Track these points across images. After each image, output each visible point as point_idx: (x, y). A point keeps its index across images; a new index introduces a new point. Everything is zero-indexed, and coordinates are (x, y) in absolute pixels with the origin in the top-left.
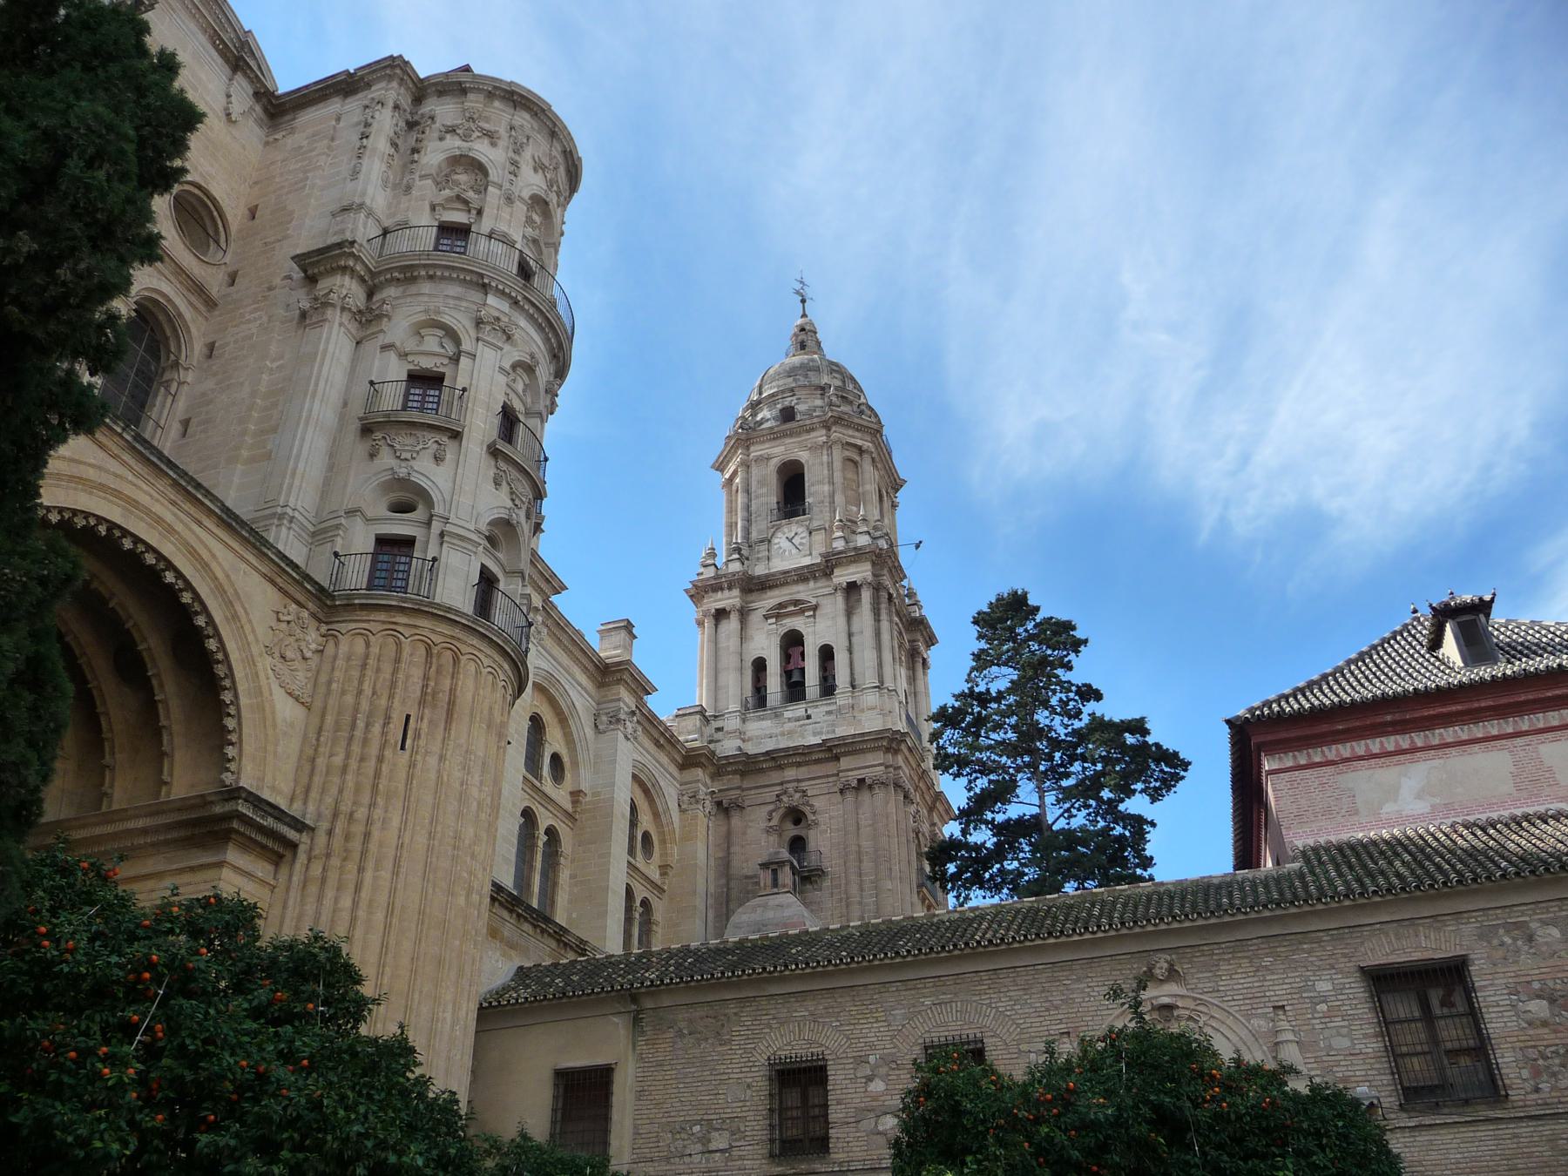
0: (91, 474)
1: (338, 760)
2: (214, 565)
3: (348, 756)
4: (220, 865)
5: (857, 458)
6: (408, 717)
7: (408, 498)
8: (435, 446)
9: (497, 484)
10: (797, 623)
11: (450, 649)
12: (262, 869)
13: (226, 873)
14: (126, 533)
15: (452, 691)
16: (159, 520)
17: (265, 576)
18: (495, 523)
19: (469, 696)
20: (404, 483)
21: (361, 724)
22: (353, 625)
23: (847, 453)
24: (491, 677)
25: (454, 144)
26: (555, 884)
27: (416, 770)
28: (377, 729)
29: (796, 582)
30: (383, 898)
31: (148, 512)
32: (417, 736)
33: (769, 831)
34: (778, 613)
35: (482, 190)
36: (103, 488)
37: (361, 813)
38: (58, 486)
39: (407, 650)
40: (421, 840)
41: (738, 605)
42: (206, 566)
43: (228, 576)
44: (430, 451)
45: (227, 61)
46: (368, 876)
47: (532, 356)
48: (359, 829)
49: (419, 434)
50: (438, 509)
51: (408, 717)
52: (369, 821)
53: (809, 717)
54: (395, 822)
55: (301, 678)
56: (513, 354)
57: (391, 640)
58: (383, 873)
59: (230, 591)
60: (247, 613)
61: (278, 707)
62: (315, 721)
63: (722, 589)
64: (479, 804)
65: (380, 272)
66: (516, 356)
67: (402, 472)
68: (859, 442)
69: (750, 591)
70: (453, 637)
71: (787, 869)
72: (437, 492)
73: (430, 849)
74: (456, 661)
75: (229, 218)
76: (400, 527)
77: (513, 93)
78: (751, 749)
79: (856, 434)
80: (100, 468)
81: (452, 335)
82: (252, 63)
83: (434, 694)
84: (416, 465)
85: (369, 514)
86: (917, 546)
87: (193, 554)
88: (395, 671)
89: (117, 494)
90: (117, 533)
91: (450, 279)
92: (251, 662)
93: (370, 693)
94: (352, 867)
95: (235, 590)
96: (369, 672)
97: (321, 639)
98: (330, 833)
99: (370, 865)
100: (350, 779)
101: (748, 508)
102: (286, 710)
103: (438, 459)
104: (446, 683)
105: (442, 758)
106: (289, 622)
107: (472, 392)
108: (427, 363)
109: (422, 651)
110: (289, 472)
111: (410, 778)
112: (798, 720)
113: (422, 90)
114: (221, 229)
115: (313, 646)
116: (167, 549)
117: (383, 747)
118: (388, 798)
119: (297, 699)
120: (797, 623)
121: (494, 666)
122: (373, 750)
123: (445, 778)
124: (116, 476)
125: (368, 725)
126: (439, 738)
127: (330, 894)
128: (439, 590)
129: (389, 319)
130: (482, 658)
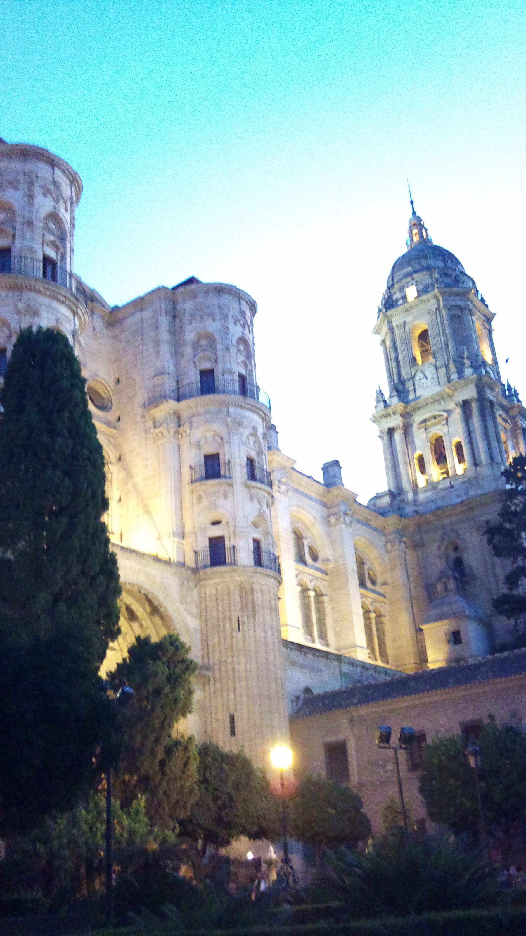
1: (216, 640)
3: (219, 637)
5: (459, 313)
9: (251, 499)
19: (260, 600)
21: (221, 624)
23: (453, 312)
26: (324, 615)
28: (228, 625)
32: (244, 623)
33: (439, 556)
37: (229, 660)
41: (401, 425)
48: (230, 667)
52: (233, 663)
53: (452, 487)
55: (195, 610)
63: (389, 415)
68: (459, 303)
71: (452, 581)
78: (421, 509)
79: (457, 298)
86: (507, 361)
88: (229, 599)
101: (397, 358)
103: (226, 496)
104: (250, 598)
105: (255, 630)
107: (232, 461)
108: (211, 450)
111: (244, 642)
112: (446, 489)
117: (231, 632)
125: (224, 623)
126: (252, 622)
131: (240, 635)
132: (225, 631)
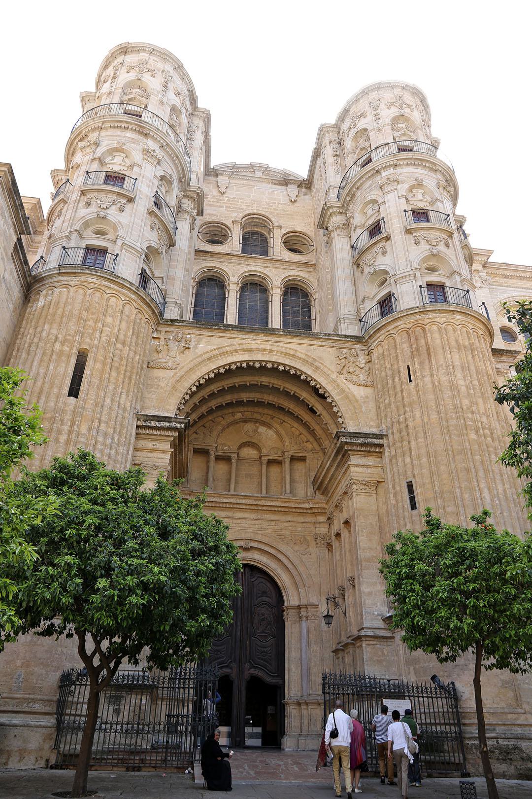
0: (228, 349)
1: (387, 401)
2: (298, 354)
4: (349, 467)
6: (408, 367)
7: (382, 278)
8: (381, 249)
9: (417, 243)
11: (418, 326)
12: (371, 461)
13: (352, 469)
14: (254, 362)
15: (427, 343)
16: (265, 350)
17: (326, 346)
18: (426, 259)
19: (438, 341)
20: (375, 273)
21: (390, 381)
22: (375, 344)
24: (450, 327)
25: (352, 133)
27: (419, 387)
28: (397, 379)
30: (423, 451)
31: (258, 350)
32: (415, 372)
36: (235, 351)
37: (402, 418)
38: (218, 359)
39: (398, 339)
42: (294, 356)
43: (307, 355)
44: (380, 253)
45: (282, 185)
46: (413, 444)
47: (416, 179)
48: (403, 426)
49: (373, 250)
51: (408, 367)
54: (418, 414)
55: (362, 378)
56: (403, 188)
57: (390, 339)
58: (419, 440)
59: (310, 360)
60: (322, 364)
61: (355, 393)
62: (376, 390)
64: (467, 387)
65: (343, 205)
66: (406, 186)
70: (416, 321)
72: (388, 267)
73: (441, 419)
74: (424, 330)
75: (309, 233)
76: (383, 293)
77: (363, 91)
80: (231, 345)
81: (374, 202)
82: (291, 178)
83: (418, 350)
84: (376, 264)
85: (372, 296)
87: (286, 354)
89: (242, 350)
90: (251, 363)
91: (364, 182)
92: (334, 381)
93: (390, 367)
94: (405, 443)
95: (313, 358)
96: (386, 358)
97: (367, 357)
98: (393, 433)
99: (412, 439)
102: (359, 392)
104: (423, 342)
105: (432, 375)
106: (346, 358)
108: (370, 222)
109: (405, 335)
110: (339, 303)
111: (418, 391)
113: (337, 127)
114: (308, 239)
115: (364, 361)
116: (274, 358)
118: (411, 404)
119: (364, 385)
121: (449, 320)
122: (399, 389)
123: (437, 384)
124: (239, 344)
125: (393, 379)
126: (427, 367)
127: (400, 460)
128: (401, 306)
129: (353, 217)
130: (439, 321)
132: (394, 387)
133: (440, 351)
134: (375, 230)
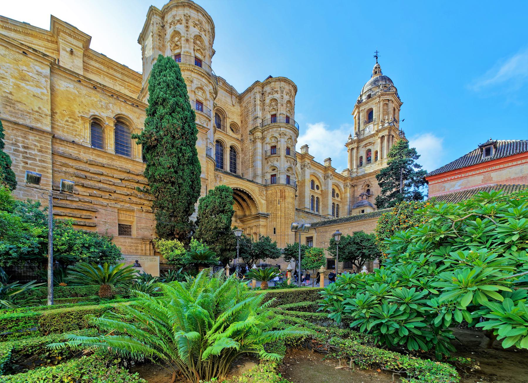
10: (369, 147)
29: (370, 138)
34: (365, 146)
35: (277, 105)
37: (275, 213)
40: (283, 214)
50: (279, 169)
52: (276, 213)
54: (279, 213)
67: (272, 165)
69: (359, 142)
74: (285, 191)
92: (257, 197)
100: (273, 209)
118: (278, 210)
120: (369, 147)
122: (275, 205)
131: (279, 205)
133: (287, 198)
134: (274, 148)
